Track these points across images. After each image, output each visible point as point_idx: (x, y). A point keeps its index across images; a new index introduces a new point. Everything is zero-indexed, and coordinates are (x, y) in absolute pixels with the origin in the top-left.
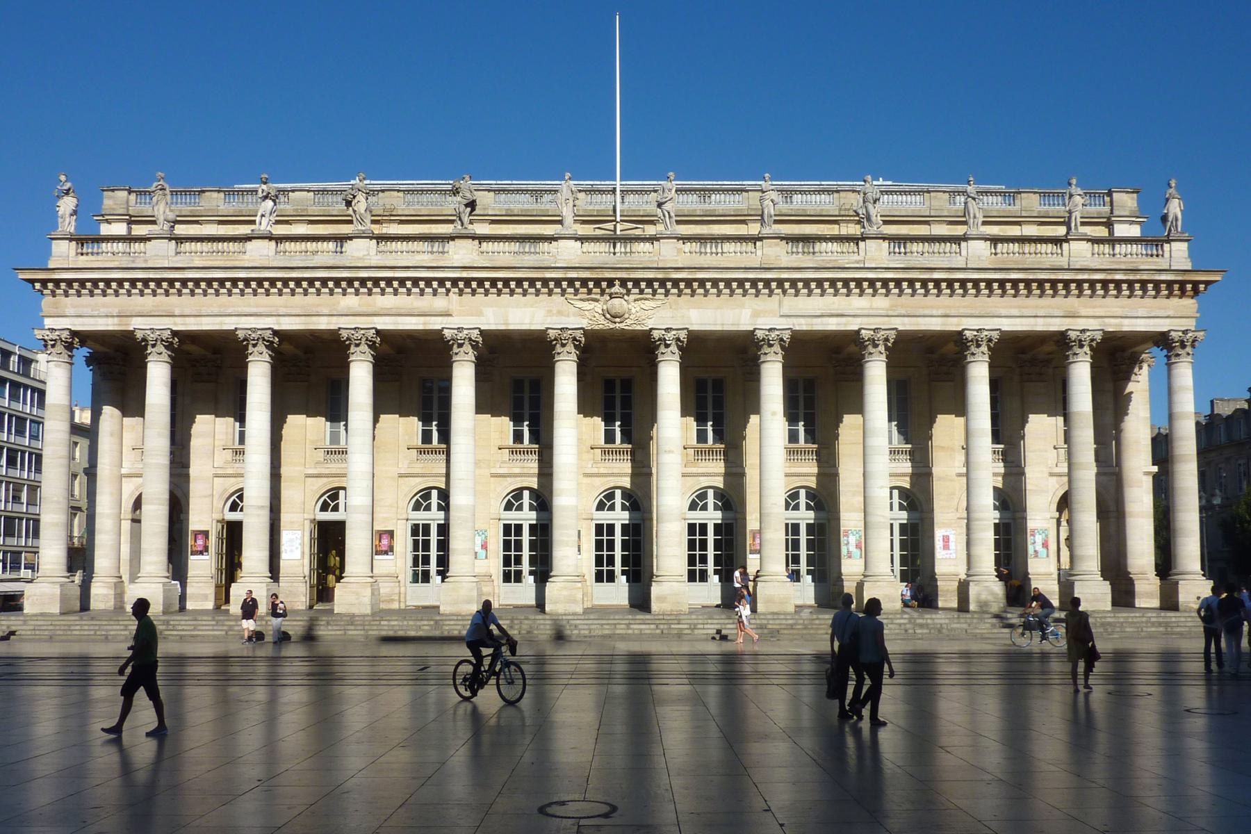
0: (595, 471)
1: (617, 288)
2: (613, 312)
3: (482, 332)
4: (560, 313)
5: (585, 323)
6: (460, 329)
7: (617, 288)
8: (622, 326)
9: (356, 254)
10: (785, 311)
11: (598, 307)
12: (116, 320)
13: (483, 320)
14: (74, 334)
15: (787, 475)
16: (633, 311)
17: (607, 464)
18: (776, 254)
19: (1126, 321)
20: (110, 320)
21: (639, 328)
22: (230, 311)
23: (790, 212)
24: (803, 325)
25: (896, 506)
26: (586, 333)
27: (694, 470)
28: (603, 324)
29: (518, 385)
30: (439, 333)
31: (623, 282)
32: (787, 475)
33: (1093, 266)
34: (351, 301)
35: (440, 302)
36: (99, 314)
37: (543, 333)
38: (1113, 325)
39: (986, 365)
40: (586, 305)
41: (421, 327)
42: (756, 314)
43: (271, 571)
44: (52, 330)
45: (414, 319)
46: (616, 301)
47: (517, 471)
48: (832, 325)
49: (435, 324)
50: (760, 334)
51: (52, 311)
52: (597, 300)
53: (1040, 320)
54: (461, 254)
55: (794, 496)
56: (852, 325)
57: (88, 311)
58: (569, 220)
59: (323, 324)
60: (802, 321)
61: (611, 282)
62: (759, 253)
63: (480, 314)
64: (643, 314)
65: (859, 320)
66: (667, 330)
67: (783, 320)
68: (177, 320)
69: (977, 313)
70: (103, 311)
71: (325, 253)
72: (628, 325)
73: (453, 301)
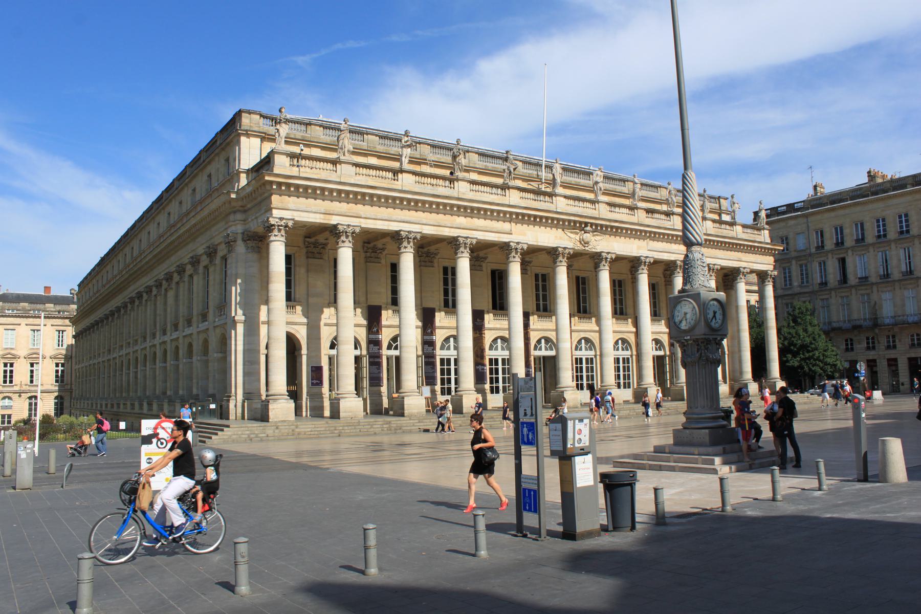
1: (588, 228)
2: (586, 240)
4: (561, 238)
5: (570, 245)
11: (577, 237)
12: (322, 216)
15: (614, 332)
18: (641, 217)
20: (318, 216)
22: (394, 218)
28: (579, 247)
29: (445, 270)
31: (592, 224)
32: (614, 332)
34: (461, 220)
35: (506, 226)
36: (310, 212)
40: (572, 236)
42: (639, 248)
43: (356, 390)
49: (505, 238)
51: (280, 206)
52: (577, 234)
54: (514, 198)
55: (616, 343)
57: (303, 207)
61: (586, 224)
70: (314, 209)
71: (442, 189)
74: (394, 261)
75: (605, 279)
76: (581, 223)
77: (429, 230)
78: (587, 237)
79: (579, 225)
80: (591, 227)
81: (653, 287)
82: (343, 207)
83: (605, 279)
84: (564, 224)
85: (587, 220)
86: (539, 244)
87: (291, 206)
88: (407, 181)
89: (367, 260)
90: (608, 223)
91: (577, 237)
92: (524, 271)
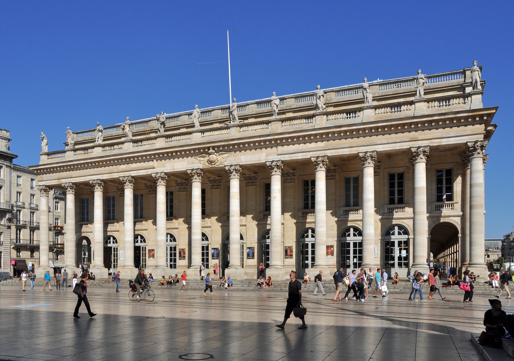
1: (211, 151)
3: (166, 174)
4: (192, 163)
5: (201, 166)
6: (157, 173)
7: (211, 151)
8: (215, 166)
9: (126, 148)
10: (279, 152)
13: (166, 168)
14: (46, 186)
16: (219, 159)
21: (221, 166)
23: (304, 105)
24: (287, 158)
25: (169, 240)
28: (208, 166)
30: (150, 176)
33: (426, 113)
35: (151, 164)
38: (435, 143)
39: (373, 168)
41: (145, 174)
42: (268, 155)
44: (40, 186)
45: (143, 171)
46: (211, 156)
48: (300, 156)
49: (149, 172)
50: (268, 164)
56: (307, 156)
58: (197, 124)
59: (115, 176)
60: (287, 156)
61: (209, 148)
62: (270, 128)
63: (165, 166)
64: (223, 160)
65: (311, 153)
66: (231, 166)
68: (74, 179)
69: (366, 144)
73: (155, 163)
74: (268, 182)
76: (204, 149)
78: (213, 157)
79: (202, 151)
80: (214, 149)
81: (136, 198)
82: (65, 174)
84: (185, 153)
85: (208, 145)
86: (176, 170)
87: (45, 179)
88: (321, 122)
89: (247, 185)
90: (226, 143)
91: (206, 159)
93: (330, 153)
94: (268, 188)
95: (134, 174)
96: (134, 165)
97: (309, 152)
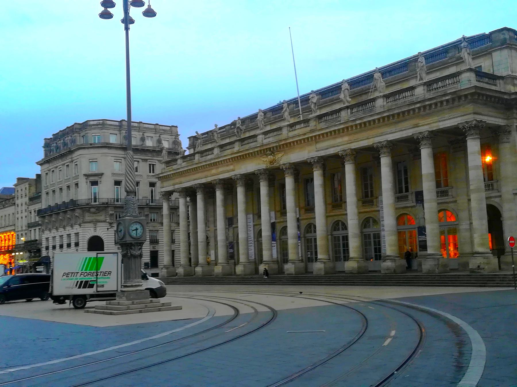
0: (305, 217)
4: (259, 164)
7: (268, 152)
17: (306, 215)
19: (441, 123)
24: (322, 153)
26: (265, 170)
27: (332, 214)
28: (269, 166)
31: (270, 148)
37: (253, 174)
42: (309, 152)
47: (282, 220)
53: (404, 132)
60: (323, 152)
67: (317, 153)
72: (276, 165)
75: (289, 182)
77: (203, 181)
83: (289, 182)
86: (249, 172)
92: (296, 180)
93: (354, 146)
94: (283, 186)
95: (221, 176)
96: (221, 170)
97: (338, 146)
